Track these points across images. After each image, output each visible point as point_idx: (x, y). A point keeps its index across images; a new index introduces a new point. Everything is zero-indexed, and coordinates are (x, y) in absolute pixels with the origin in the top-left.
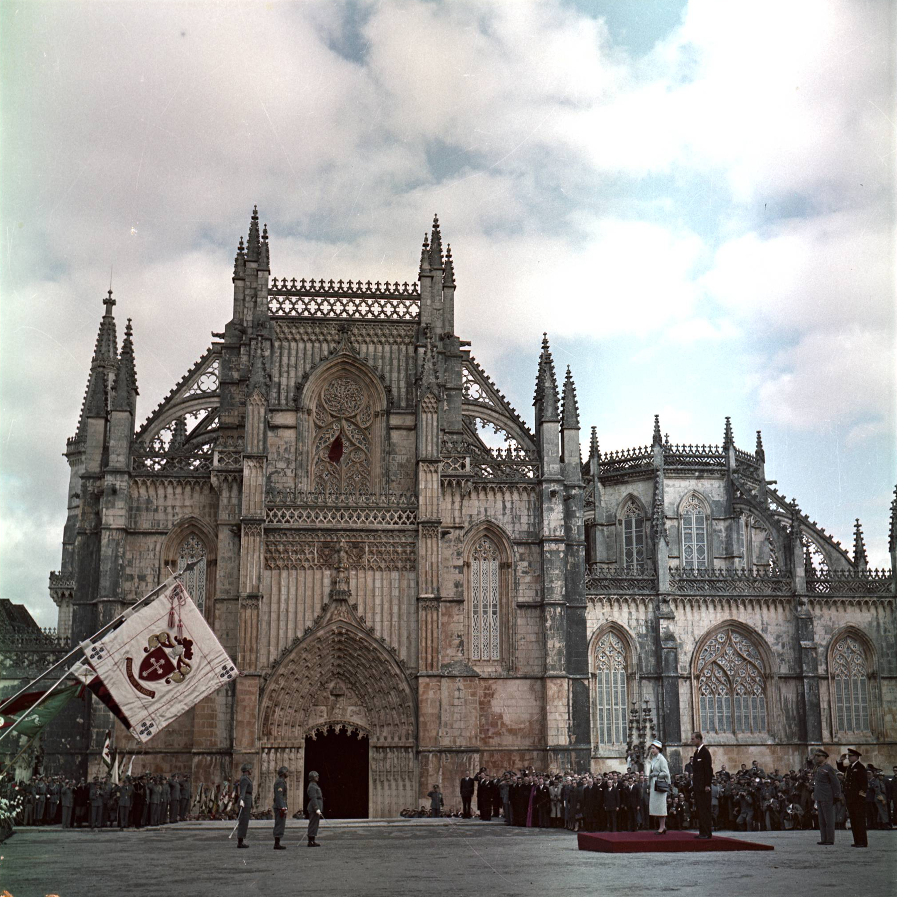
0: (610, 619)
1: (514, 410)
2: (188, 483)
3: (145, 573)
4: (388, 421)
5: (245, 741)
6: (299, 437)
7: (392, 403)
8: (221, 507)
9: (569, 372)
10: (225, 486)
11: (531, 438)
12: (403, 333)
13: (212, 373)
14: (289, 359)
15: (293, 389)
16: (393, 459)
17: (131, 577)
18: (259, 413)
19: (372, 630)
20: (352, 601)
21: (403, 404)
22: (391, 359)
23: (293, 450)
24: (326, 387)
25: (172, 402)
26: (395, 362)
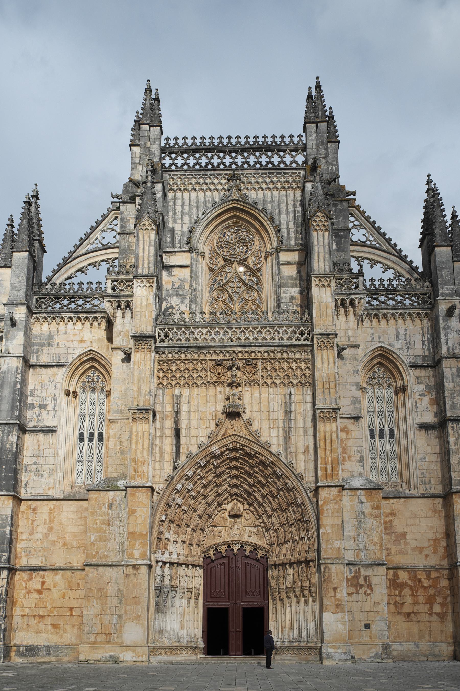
2: (87, 318)
3: (46, 402)
7: (282, 243)
17: (32, 406)
19: (268, 444)
20: (245, 416)
23: (187, 287)
26: (283, 206)
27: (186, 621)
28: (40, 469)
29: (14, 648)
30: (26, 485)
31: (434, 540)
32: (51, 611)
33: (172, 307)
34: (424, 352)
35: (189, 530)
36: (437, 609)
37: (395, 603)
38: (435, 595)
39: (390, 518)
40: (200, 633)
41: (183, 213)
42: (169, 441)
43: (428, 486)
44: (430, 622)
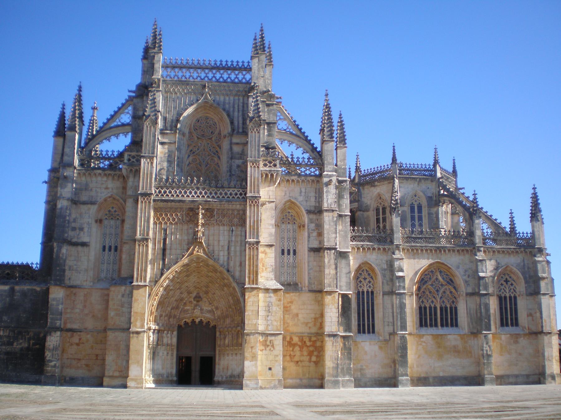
0: (365, 259)
1: (307, 137)
4: (231, 140)
8: (128, 188)
9: (340, 115)
10: (131, 176)
11: (319, 152)
12: (241, 89)
13: (128, 113)
16: (234, 162)
21: (241, 130)
22: (234, 105)
24: (194, 120)
25: (102, 130)
26: (236, 106)
30: (70, 279)
31: (315, 319)
35: (169, 309)
36: (314, 359)
38: (313, 351)
39: (290, 304)
43: (313, 286)
44: (309, 367)
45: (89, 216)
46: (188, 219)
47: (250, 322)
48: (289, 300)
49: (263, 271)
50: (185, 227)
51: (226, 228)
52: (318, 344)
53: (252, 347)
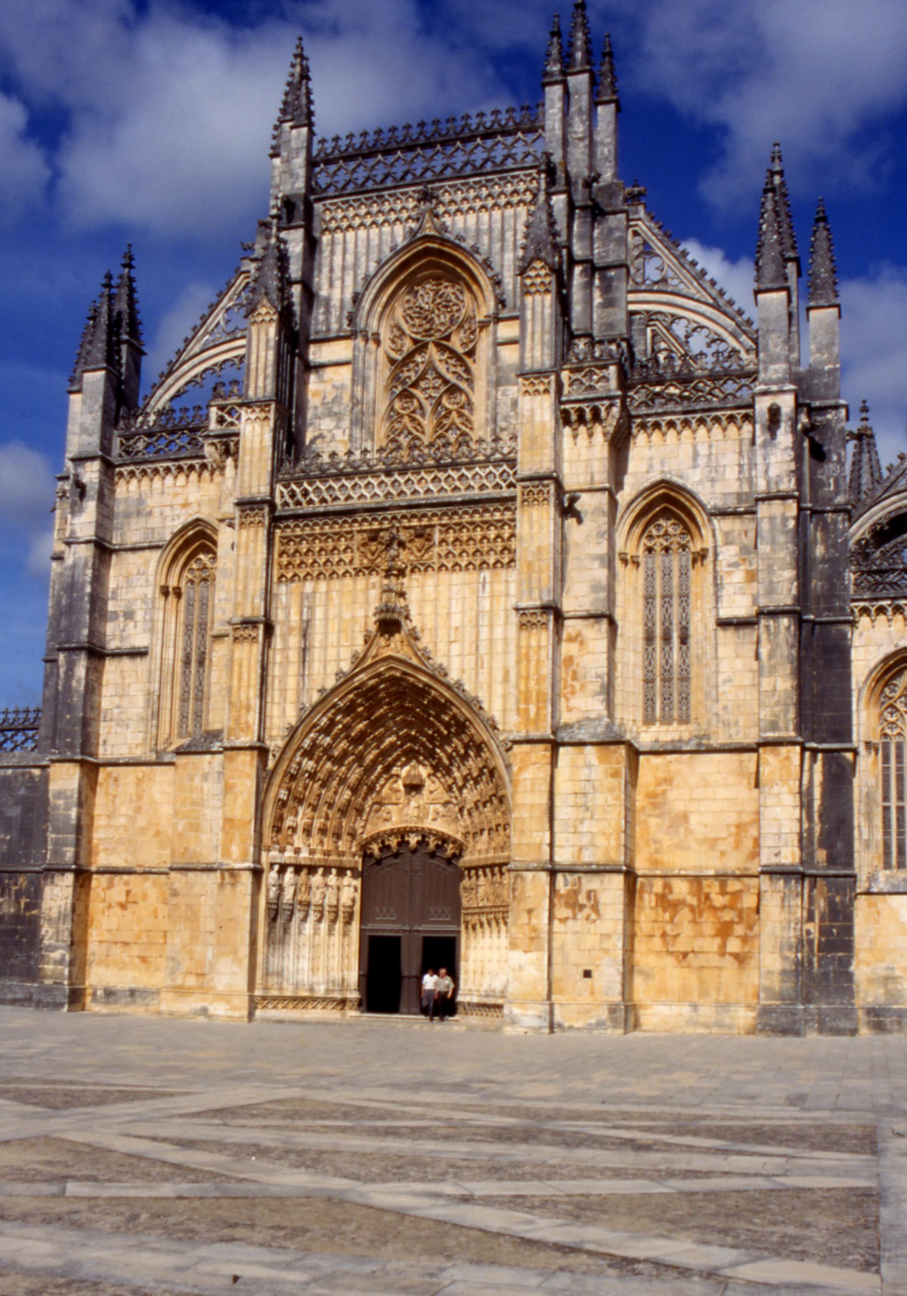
5: (235, 851)
6: (359, 378)
14: (344, 259)
15: (349, 306)
16: (504, 394)
18: (267, 334)
23: (346, 399)
26: (509, 235)
27: (326, 958)
28: (124, 717)
29: (89, 991)
30: (105, 742)
31: (738, 826)
32: (139, 936)
33: (321, 436)
34: (741, 486)
37: (664, 935)
38: (732, 923)
39: (664, 787)
40: (353, 976)
41: (344, 268)
42: (293, 669)
43: (733, 731)
45: (147, 581)
46: (365, 561)
47: (524, 841)
48: (661, 775)
49: (573, 693)
50: (361, 582)
51: (469, 576)
52: (749, 901)
53: (530, 912)
